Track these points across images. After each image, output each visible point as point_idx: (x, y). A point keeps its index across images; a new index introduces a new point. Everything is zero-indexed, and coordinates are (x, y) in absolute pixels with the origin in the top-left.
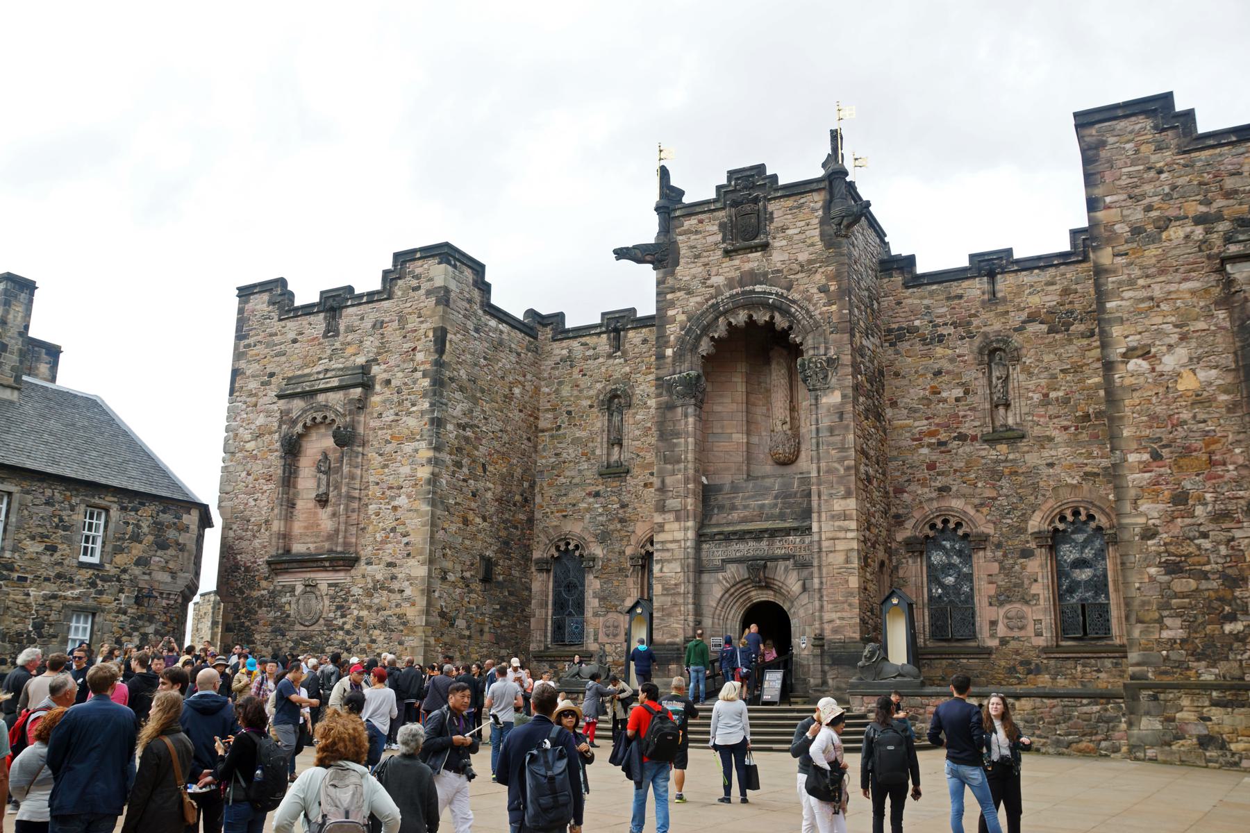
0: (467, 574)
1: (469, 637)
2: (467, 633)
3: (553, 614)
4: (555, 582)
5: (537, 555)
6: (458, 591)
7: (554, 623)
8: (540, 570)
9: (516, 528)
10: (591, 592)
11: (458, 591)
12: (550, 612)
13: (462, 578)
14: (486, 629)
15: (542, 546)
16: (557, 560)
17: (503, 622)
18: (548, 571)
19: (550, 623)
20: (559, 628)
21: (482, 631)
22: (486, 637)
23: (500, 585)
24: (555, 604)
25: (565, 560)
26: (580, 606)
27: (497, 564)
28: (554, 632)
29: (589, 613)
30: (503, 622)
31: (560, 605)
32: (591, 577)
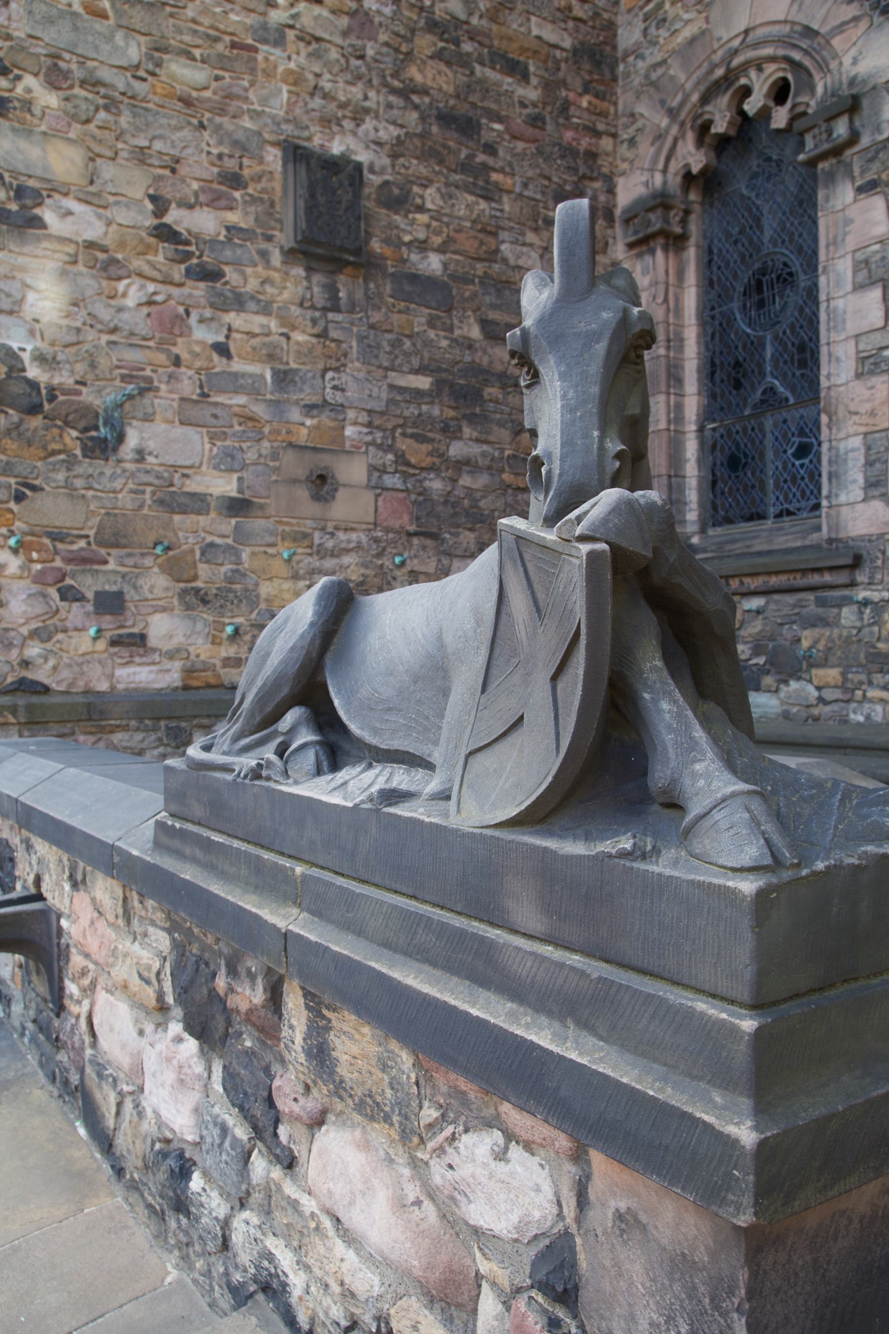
0: (204, 222)
1: (238, 506)
2: (224, 486)
3: (707, 415)
4: (708, 284)
5: (629, 191)
6: (133, 293)
7: (708, 447)
8: (641, 244)
9: (515, 69)
10: (844, 267)
11: (133, 293)
12: (692, 406)
13: (166, 234)
14: (353, 471)
15: (646, 150)
16: (706, 182)
17: (456, 450)
18: (675, 242)
19: (691, 448)
20: (735, 463)
21: (322, 484)
22: (353, 505)
23: (416, 287)
24: (711, 370)
25: (741, 186)
26: (805, 355)
27: (398, 200)
28: (712, 484)
29: (838, 367)
30: (456, 450)
31: (728, 373)
32: (845, 193)
